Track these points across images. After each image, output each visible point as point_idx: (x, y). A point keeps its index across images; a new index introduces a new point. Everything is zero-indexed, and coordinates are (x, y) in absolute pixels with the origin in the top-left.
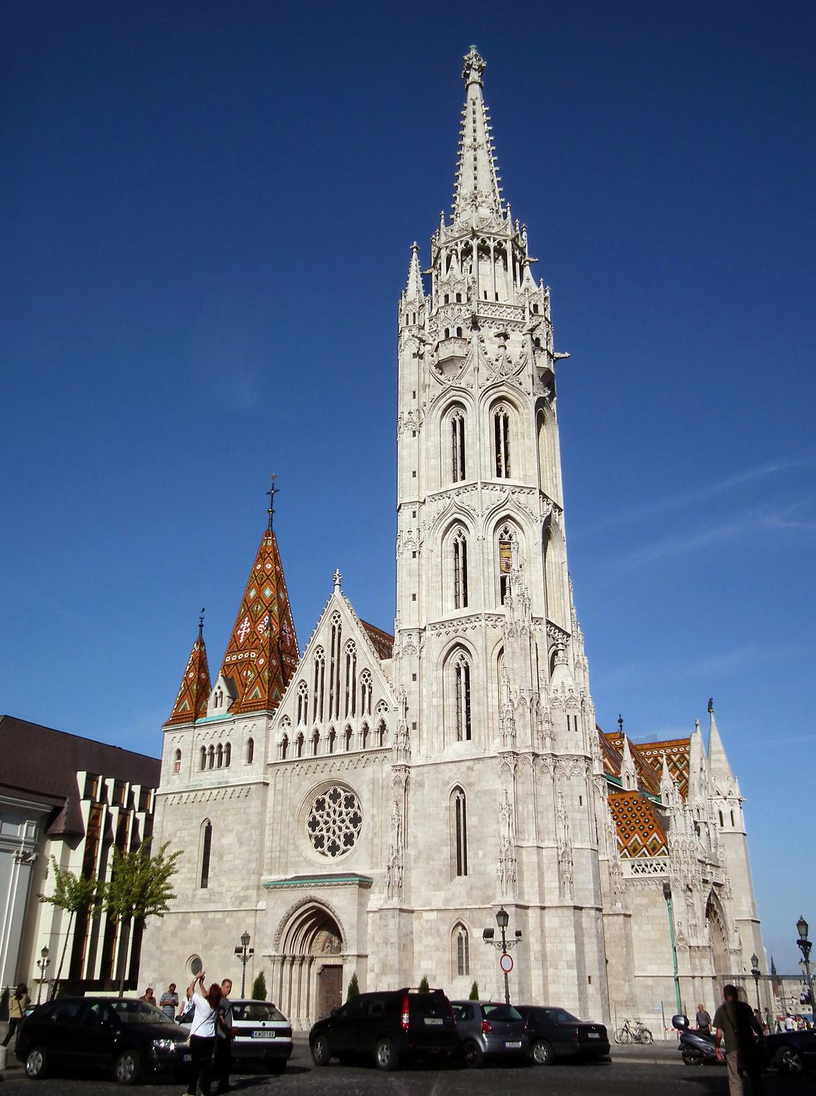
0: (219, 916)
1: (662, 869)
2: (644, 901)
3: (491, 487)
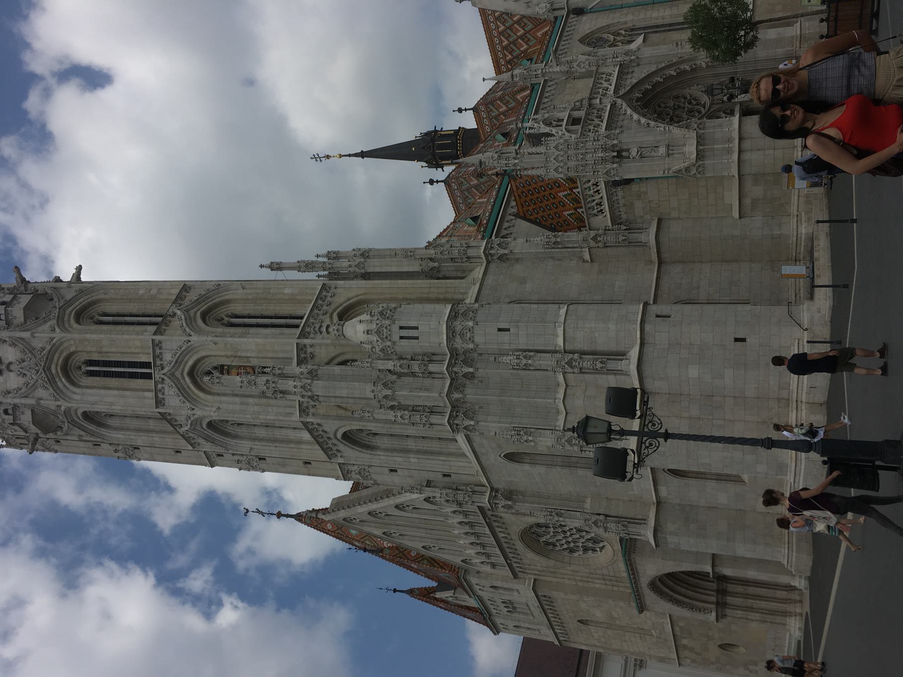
0: (677, 629)
1: (596, 184)
2: (638, 204)
3: (160, 396)
